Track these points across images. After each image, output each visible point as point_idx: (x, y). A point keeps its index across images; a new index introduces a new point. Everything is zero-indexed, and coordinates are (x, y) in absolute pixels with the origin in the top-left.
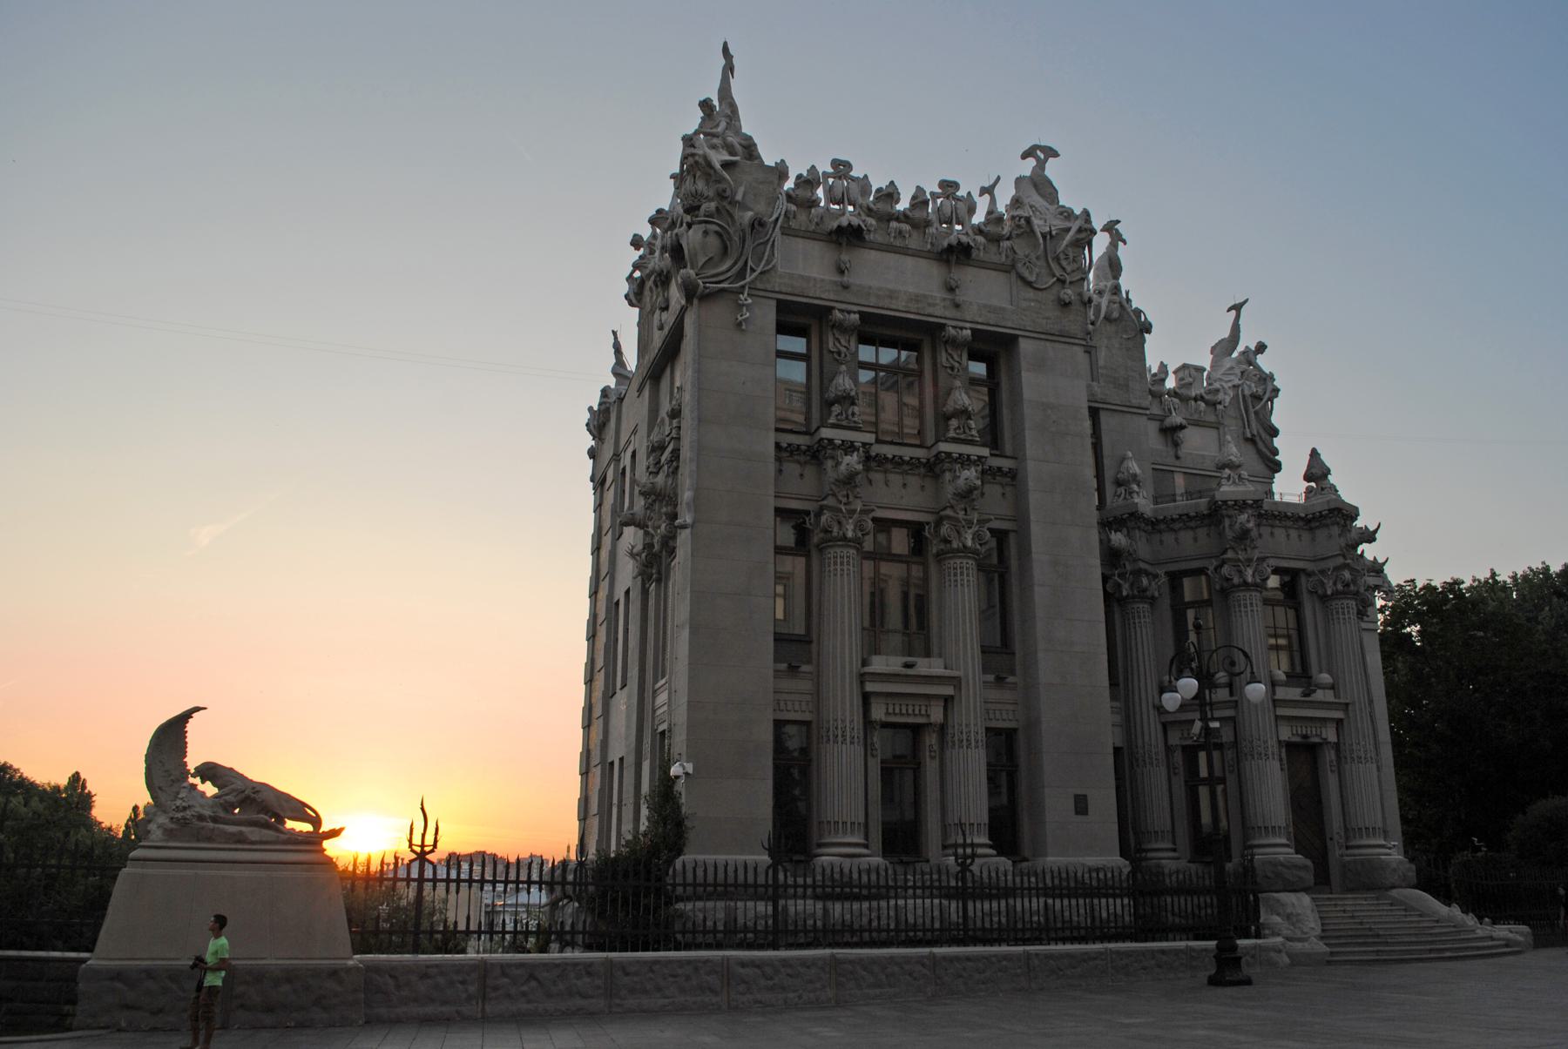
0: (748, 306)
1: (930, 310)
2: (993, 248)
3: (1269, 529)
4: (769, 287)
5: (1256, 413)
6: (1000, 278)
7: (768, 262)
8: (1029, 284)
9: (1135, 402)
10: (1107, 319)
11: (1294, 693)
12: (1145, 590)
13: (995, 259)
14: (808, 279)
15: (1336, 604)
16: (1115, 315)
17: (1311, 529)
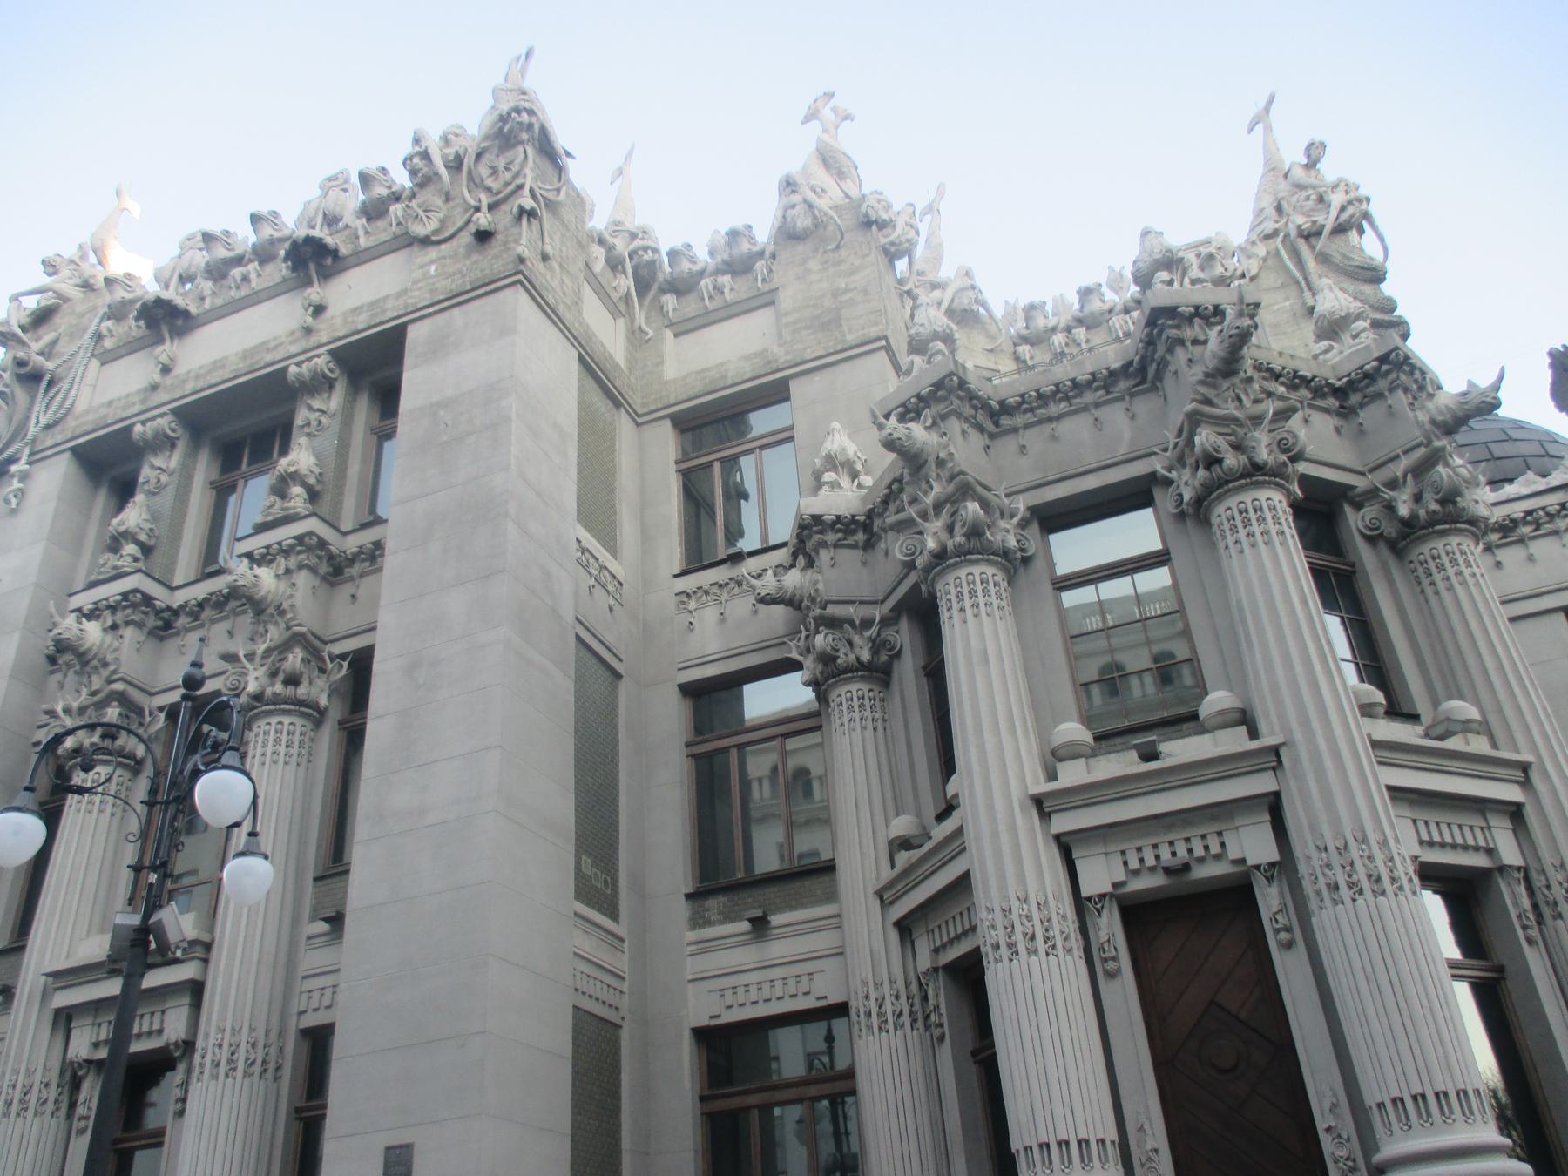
0: (24, 477)
1: (269, 358)
2: (381, 224)
4: (59, 438)
5: (1323, 259)
6: (401, 256)
7: (61, 406)
8: (425, 242)
9: (851, 338)
10: (788, 235)
12: (827, 659)
13: (384, 237)
14: (110, 403)
15: (1220, 512)
16: (803, 222)
17: (1154, 388)
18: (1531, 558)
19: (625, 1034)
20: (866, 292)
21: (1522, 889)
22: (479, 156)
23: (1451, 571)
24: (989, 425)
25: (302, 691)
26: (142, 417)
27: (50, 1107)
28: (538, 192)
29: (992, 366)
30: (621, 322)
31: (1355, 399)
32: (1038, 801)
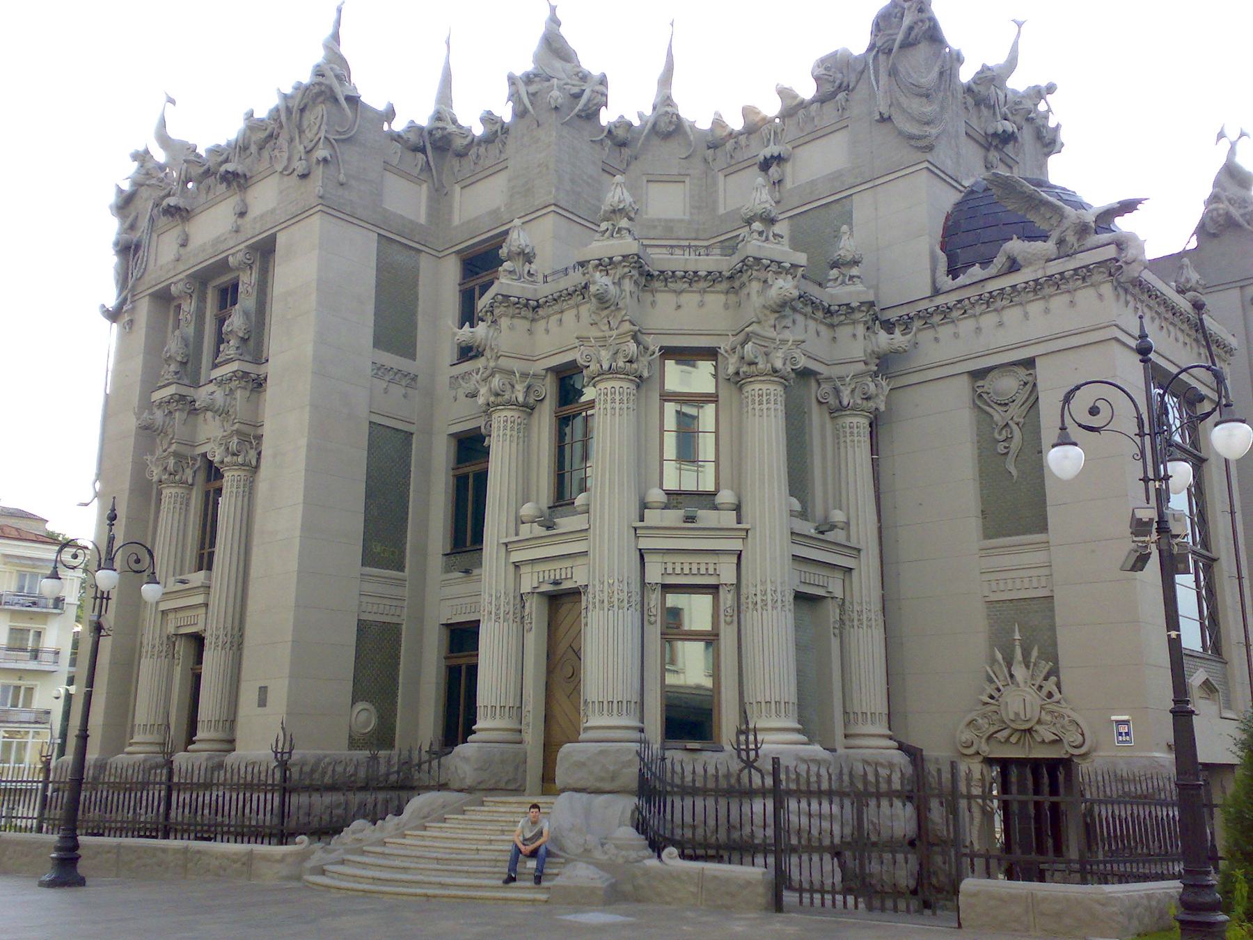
3: (559, 316)
5: (893, 73)
9: (538, 202)
11: (539, 531)
18: (956, 335)
19: (404, 627)
20: (547, 167)
21: (730, 596)
22: (302, 110)
23: (750, 407)
24: (530, 314)
25: (240, 460)
26: (174, 280)
27: (164, 654)
28: (331, 137)
29: (683, 172)
30: (425, 186)
31: (737, 284)
32: (506, 545)
